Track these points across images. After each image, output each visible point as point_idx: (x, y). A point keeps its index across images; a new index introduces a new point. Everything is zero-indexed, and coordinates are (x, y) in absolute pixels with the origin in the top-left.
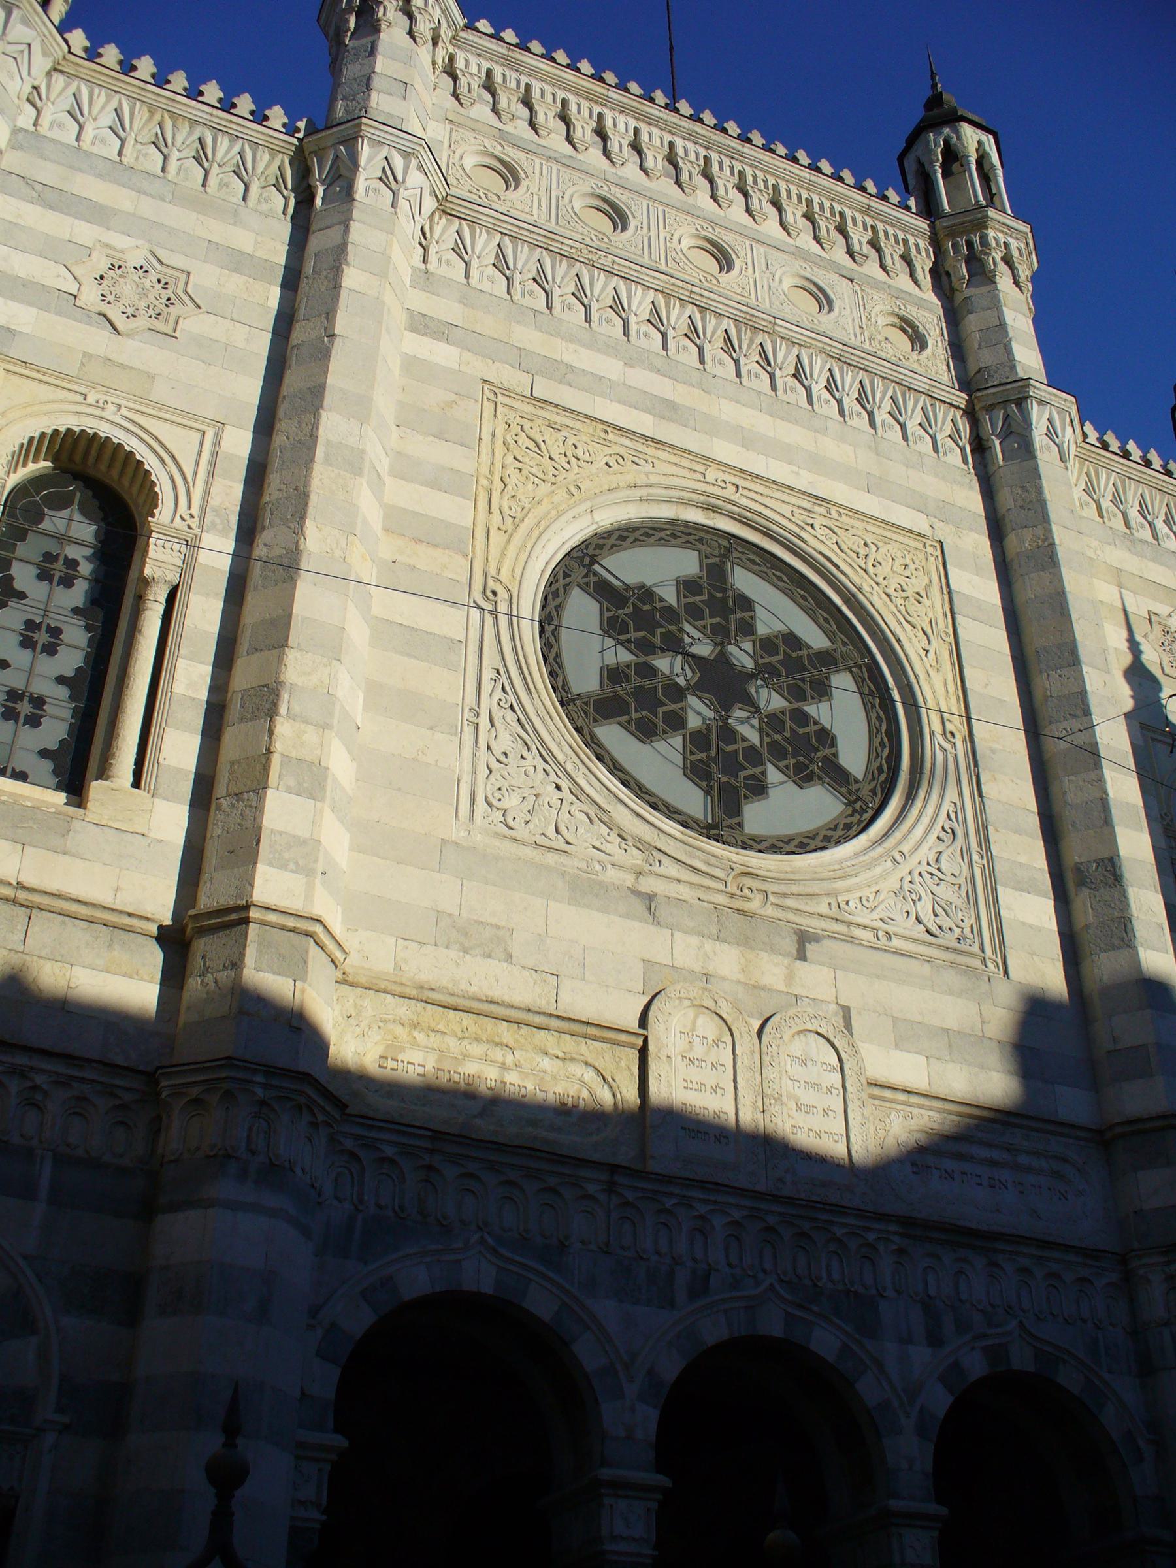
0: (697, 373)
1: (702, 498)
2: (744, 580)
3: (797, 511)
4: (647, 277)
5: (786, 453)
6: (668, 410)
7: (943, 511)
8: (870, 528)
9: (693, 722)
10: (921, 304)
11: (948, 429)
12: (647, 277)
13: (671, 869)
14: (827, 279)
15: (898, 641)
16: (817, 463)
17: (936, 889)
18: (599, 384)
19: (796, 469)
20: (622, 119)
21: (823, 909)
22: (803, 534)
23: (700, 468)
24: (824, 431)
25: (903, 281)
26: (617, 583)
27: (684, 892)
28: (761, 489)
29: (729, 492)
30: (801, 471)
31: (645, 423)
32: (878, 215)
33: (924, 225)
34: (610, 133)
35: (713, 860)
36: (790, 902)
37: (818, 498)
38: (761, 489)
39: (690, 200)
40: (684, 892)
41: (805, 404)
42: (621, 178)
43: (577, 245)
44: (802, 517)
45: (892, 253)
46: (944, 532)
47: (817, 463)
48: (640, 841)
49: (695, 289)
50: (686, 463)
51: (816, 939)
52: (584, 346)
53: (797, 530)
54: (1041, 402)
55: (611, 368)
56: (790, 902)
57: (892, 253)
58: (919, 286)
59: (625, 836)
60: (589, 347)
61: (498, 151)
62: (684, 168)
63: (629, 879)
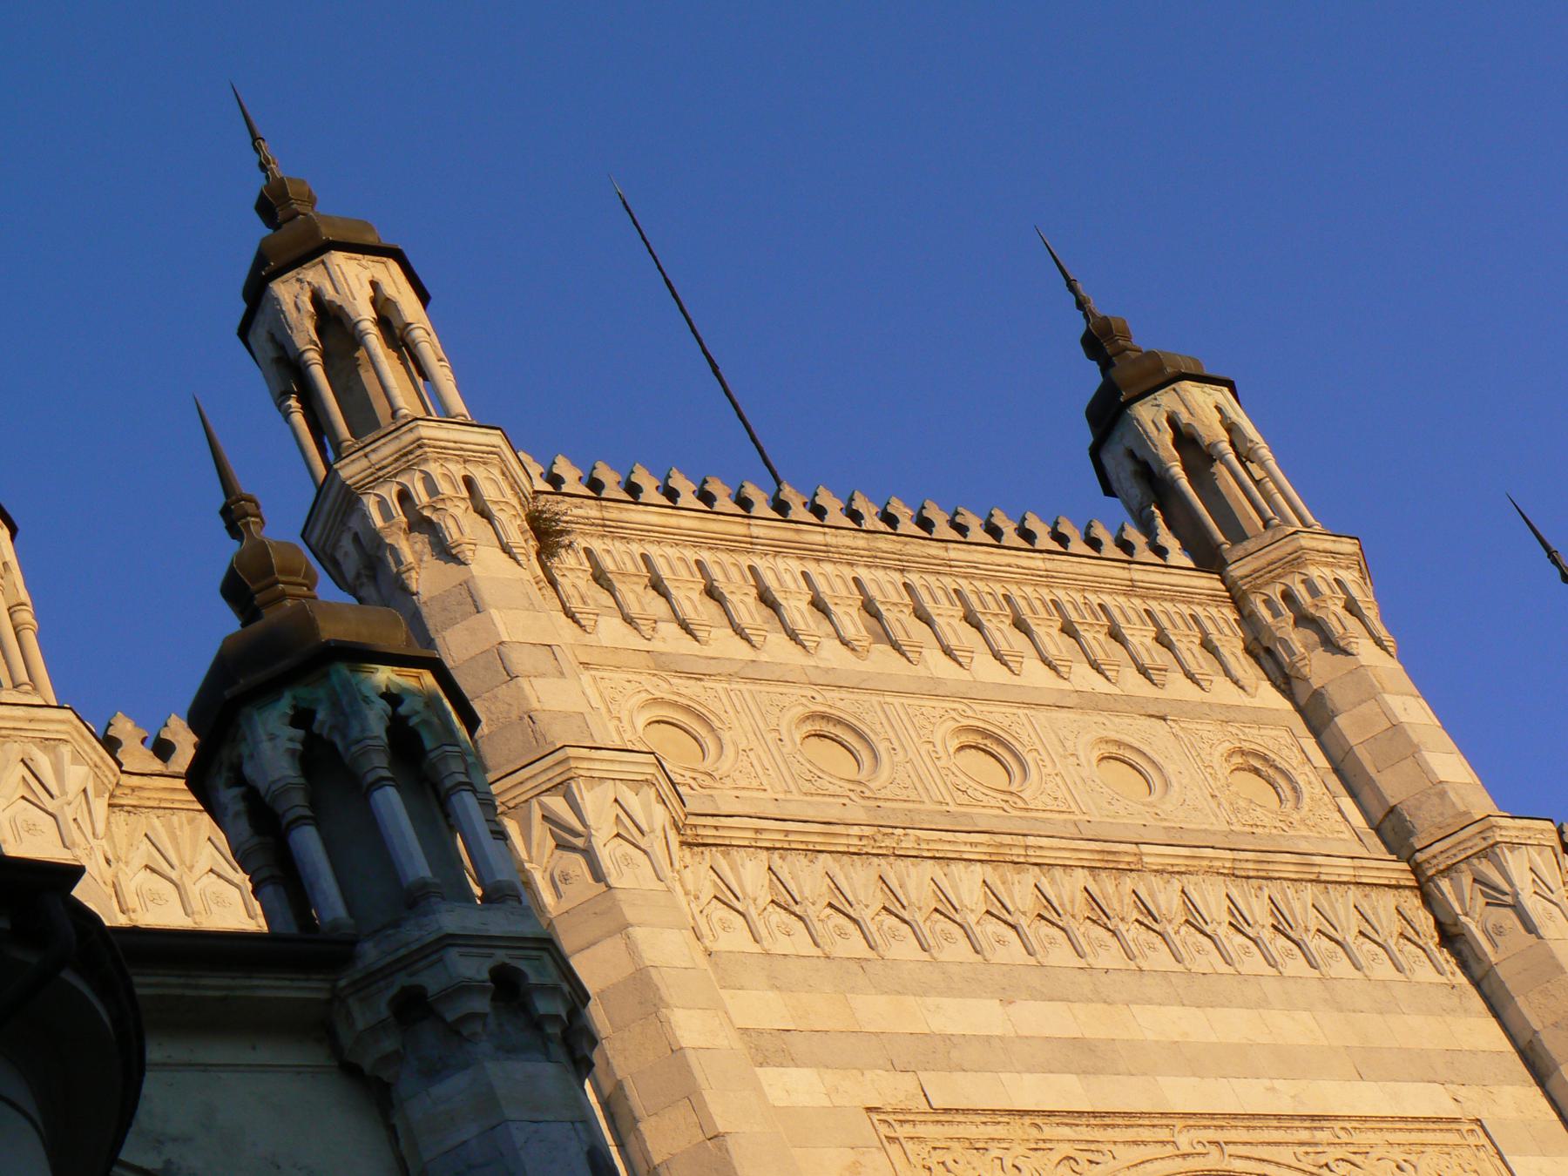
0: (1082, 977)
3: (1300, 1150)
4: (962, 844)
6: (1084, 1056)
7: (1448, 1067)
8: (1392, 1137)
10: (1259, 718)
11: (1397, 925)
12: (962, 844)
14: (1135, 730)
16: (1289, 1062)
18: (996, 1052)
19: (1267, 1083)
20: (781, 564)
23: (1163, 1134)
24: (1263, 1003)
25: (1222, 690)
28: (1243, 1135)
31: (1069, 1092)
32: (1147, 592)
33: (1207, 583)
34: (779, 597)
37: (1313, 1118)
38: (1243, 1135)
39: (920, 670)
41: (1223, 968)
42: (827, 671)
43: (868, 831)
45: (1188, 645)
46: (1474, 1103)
47: (1289, 1062)
49: (1031, 841)
50: (1146, 1134)
52: (940, 994)
54: (1513, 846)
55: (978, 1016)
57: (1188, 645)
58: (1242, 688)
60: (949, 991)
61: (663, 691)
62: (889, 615)
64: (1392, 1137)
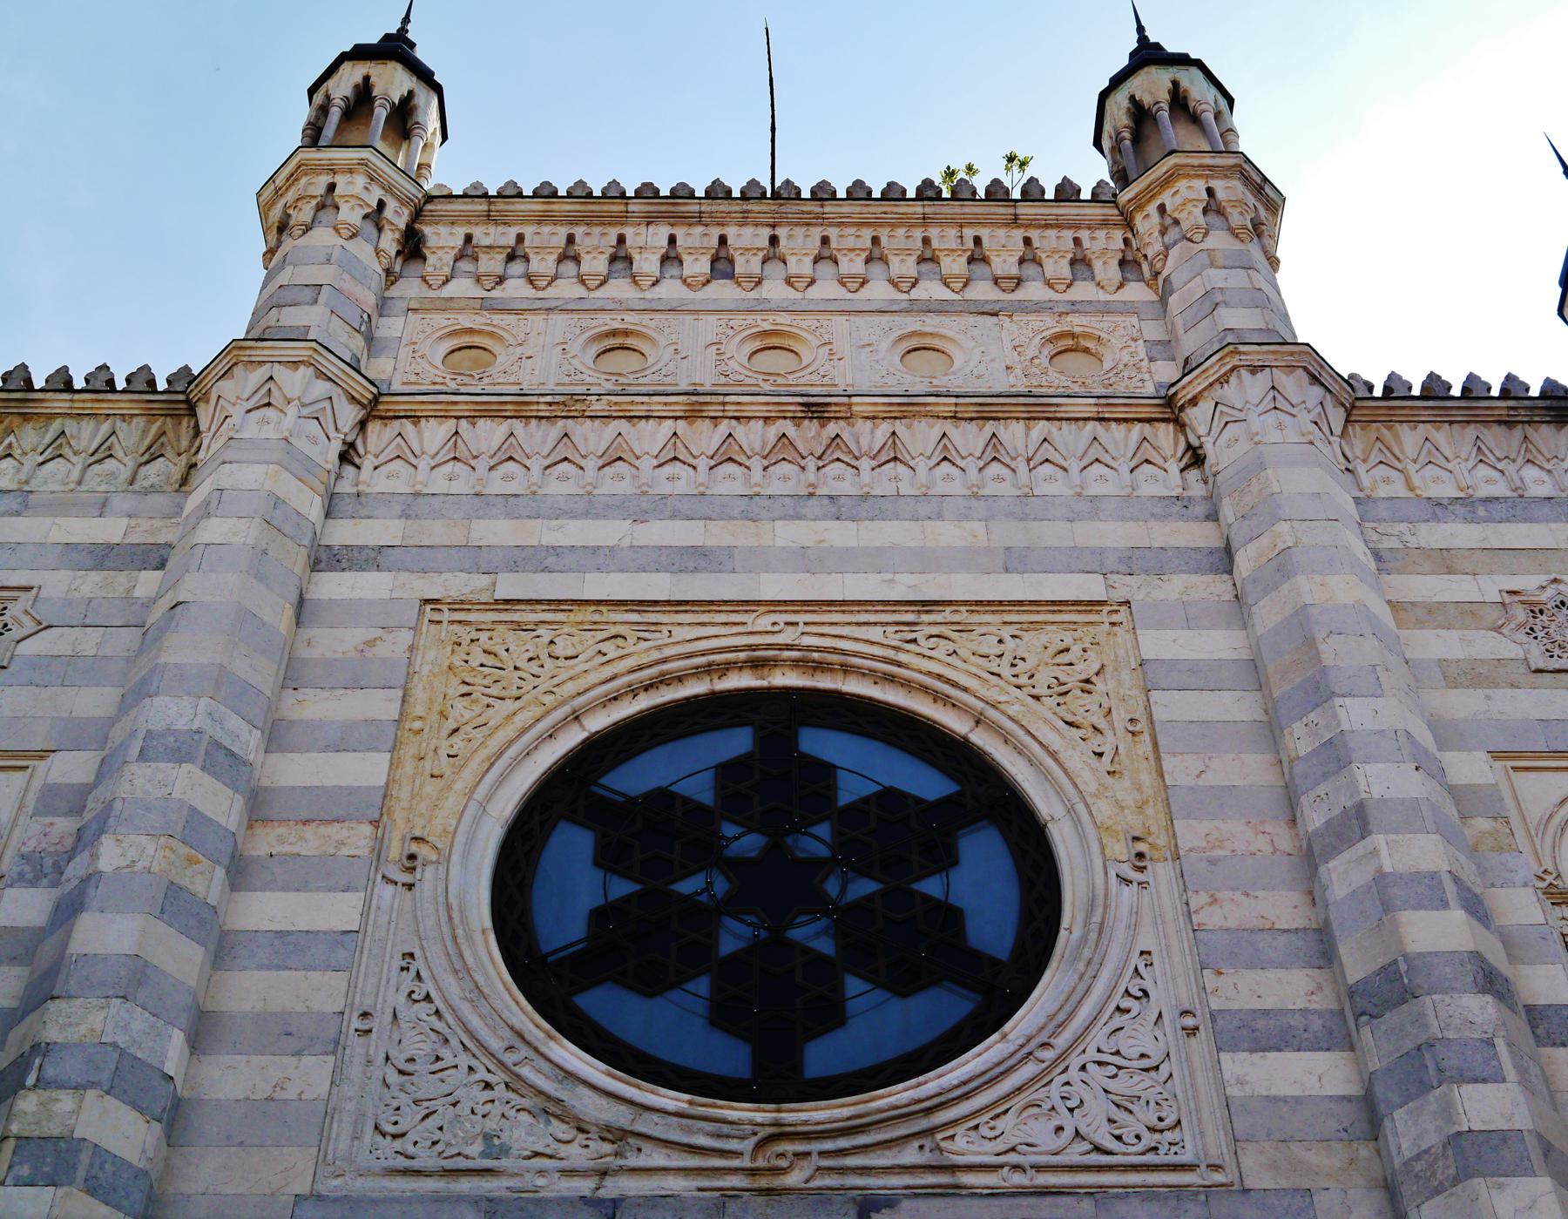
1: (742, 655)
2: (818, 743)
5: (847, 560)
6: (700, 558)
9: (728, 945)
13: (658, 1158)
15: (1053, 755)
17: (1112, 1085)
19: (889, 576)
21: (910, 1155)
22: (902, 657)
26: (621, 799)
27: (675, 1184)
29: (787, 637)
30: (898, 577)
31: (659, 586)
35: (726, 1129)
36: (850, 1161)
40: (675, 1184)
44: (898, 636)
46: (1125, 587)
47: (924, 559)
48: (608, 1128)
51: (890, 1203)
53: (890, 654)
56: (850, 1161)
59: (583, 1125)
63: (585, 1186)
64: (1008, 618)
